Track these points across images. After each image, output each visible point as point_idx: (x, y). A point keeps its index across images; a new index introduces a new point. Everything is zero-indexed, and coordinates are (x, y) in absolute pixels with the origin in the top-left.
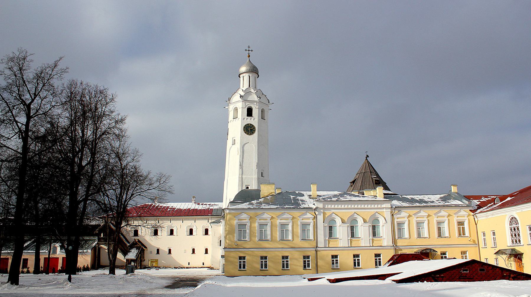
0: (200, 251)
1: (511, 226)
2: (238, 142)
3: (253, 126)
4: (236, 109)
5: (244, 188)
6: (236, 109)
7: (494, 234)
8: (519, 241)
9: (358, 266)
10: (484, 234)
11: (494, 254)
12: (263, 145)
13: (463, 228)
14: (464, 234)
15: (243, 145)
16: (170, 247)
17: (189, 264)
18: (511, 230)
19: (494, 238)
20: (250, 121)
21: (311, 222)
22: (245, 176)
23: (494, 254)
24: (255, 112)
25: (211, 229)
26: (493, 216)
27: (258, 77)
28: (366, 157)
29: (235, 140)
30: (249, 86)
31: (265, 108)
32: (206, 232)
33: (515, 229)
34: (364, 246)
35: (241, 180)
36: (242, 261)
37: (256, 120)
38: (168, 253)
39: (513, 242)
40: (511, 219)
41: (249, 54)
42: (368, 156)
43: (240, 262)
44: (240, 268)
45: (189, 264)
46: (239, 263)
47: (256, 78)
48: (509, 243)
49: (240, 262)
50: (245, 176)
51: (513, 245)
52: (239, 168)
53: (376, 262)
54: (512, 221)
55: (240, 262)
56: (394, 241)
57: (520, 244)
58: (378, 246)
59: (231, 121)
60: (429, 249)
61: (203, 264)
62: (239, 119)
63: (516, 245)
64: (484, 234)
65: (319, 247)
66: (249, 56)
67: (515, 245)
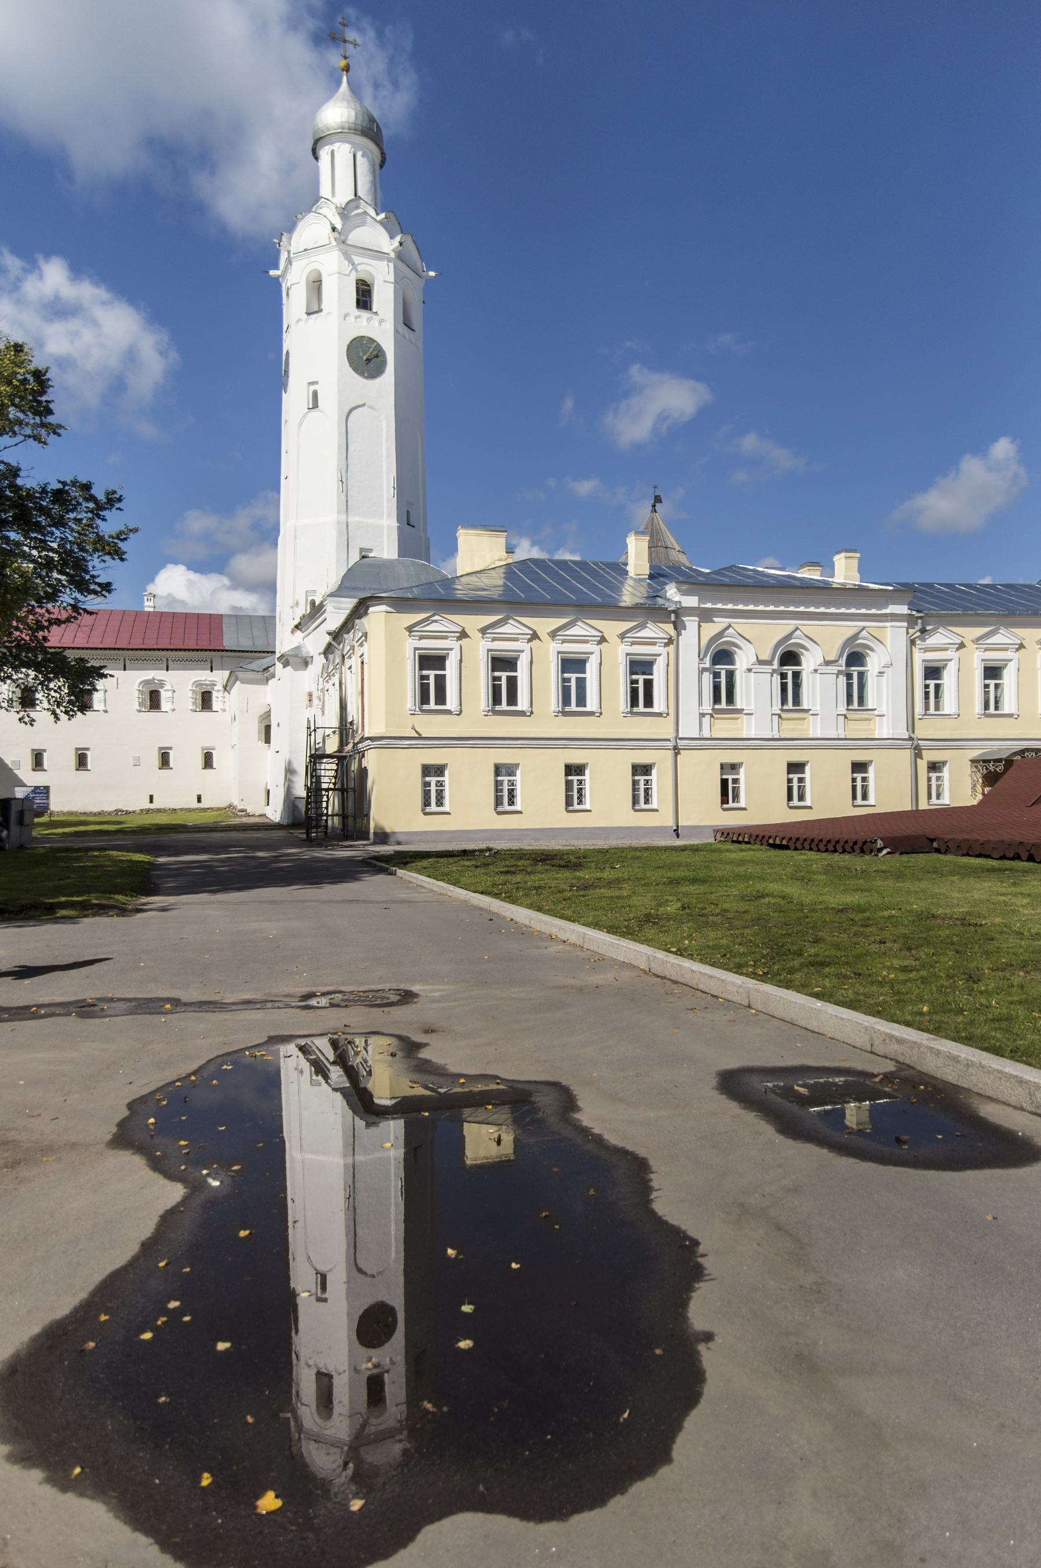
2: (329, 400)
3: (378, 346)
5: (355, 558)
15: (347, 410)
17: (151, 801)
20: (364, 325)
22: (357, 519)
24: (384, 297)
29: (315, 394)
30: (356, 195)
32: (206, 701)
34: (819, 736)
35: (346, 532)
36: (433, 780)
37: (389, 326)
45: (151, 801)
50: (357, 519)
52: (338, 489)
56: (912, 726)
59: (299, 320)
60: (1032, 750)
61: (199, 799)
62: (329, 313)
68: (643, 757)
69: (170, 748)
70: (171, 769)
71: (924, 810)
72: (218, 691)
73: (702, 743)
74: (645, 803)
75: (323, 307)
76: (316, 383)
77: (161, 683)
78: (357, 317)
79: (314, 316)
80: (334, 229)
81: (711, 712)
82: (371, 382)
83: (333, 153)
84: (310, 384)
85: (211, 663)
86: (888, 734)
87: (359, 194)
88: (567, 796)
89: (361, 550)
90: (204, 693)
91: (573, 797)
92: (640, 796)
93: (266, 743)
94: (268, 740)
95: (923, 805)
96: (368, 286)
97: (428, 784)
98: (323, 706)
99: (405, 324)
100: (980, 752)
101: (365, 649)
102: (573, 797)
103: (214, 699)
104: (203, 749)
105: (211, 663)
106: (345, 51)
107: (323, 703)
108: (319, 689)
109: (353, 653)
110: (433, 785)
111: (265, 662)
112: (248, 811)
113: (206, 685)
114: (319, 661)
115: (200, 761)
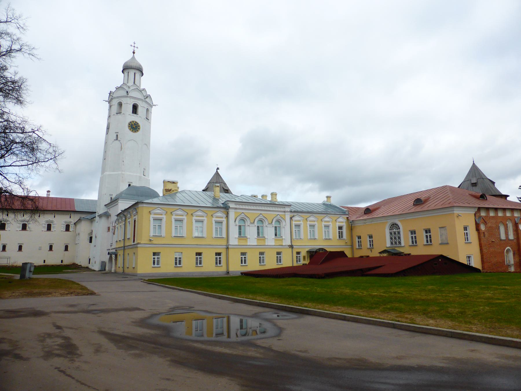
0: (59, 248)
1: (391, 231)
4: (120, 104)
6: (120, 104)
7: (371, 237)
8: (400, 243)
9: (179, 265)
10: (359, 237)
11: (379, 253)
12: (145, 144)
13: (342, 232)
14: (342, 237)
16: (52, 244)
18: (391, 233)
19: (359, 241)
21: (225, 220)
22: (128, 173)
23: (379, 253)
24: (140, 110)
25: (73, 226)
26: (372, 223)
27: (142, 76)
28: (217, 170)
29: (117, 135)
31: (149, 108)
33: (395, 233)
36: (156, 257)
38: (2, 250)
39: (392, 243)
40: (392, 225)
41: (134, 50)
42: (218, 169)
43: (153, 258)
44: (153, 265)
46: (153, 260)
47: (141, 76)
48: (388, 244)
49: (153, 258)
50: (128, 173)
51: (392, 246)
53: (277, 260)
54: (393, 227)
55: (154, 258)
57: (400, 245)
58: (279, 245)
59: (114, 115)
63: (396, 245)
64: (359, 237)
65: (230, 245)
66: (134, 53)
67: (394, 246)
68: (218, 251)
69: (53, 244)
70: (53, 251)
71: (295, 266)
72: (72, 225)
73: (236, 247)
74: (219, 264)
75: (122, 112)
76: (118, 133)
77: (52, 222)
78: (132, 115)
79: (118, 114)
80: (127, 92)
81: (238, 237)
82: (135, 134)
83: (128, 72)
84: (116, 133)
85: (70, 215)
86: (285, 244)
87: (136, 83)
88: (196, 262)
89: (128, 182)
90: (67, 225)
91: (199, 262)
92: (218, 262)
93: (90, 243)
94: (91, 242)
95: (295, 264)
96: (136, 107)
97: (154, 258)
98: (114, 232)
99: (146, 118)
100: (308, 249)
101: (136, 217)
102: (199, 262)
103: (70, 227)
104: (65, 244)
105: (70, 215)
106: (134, 49)
107: (114, 231)
108: (113, 226)
109: (131, 217)
110: (156, 258)
111: (93, 216)
112: (82, 266)
113: (68, 222)
114: (114, 218)
115: (64, 248)
